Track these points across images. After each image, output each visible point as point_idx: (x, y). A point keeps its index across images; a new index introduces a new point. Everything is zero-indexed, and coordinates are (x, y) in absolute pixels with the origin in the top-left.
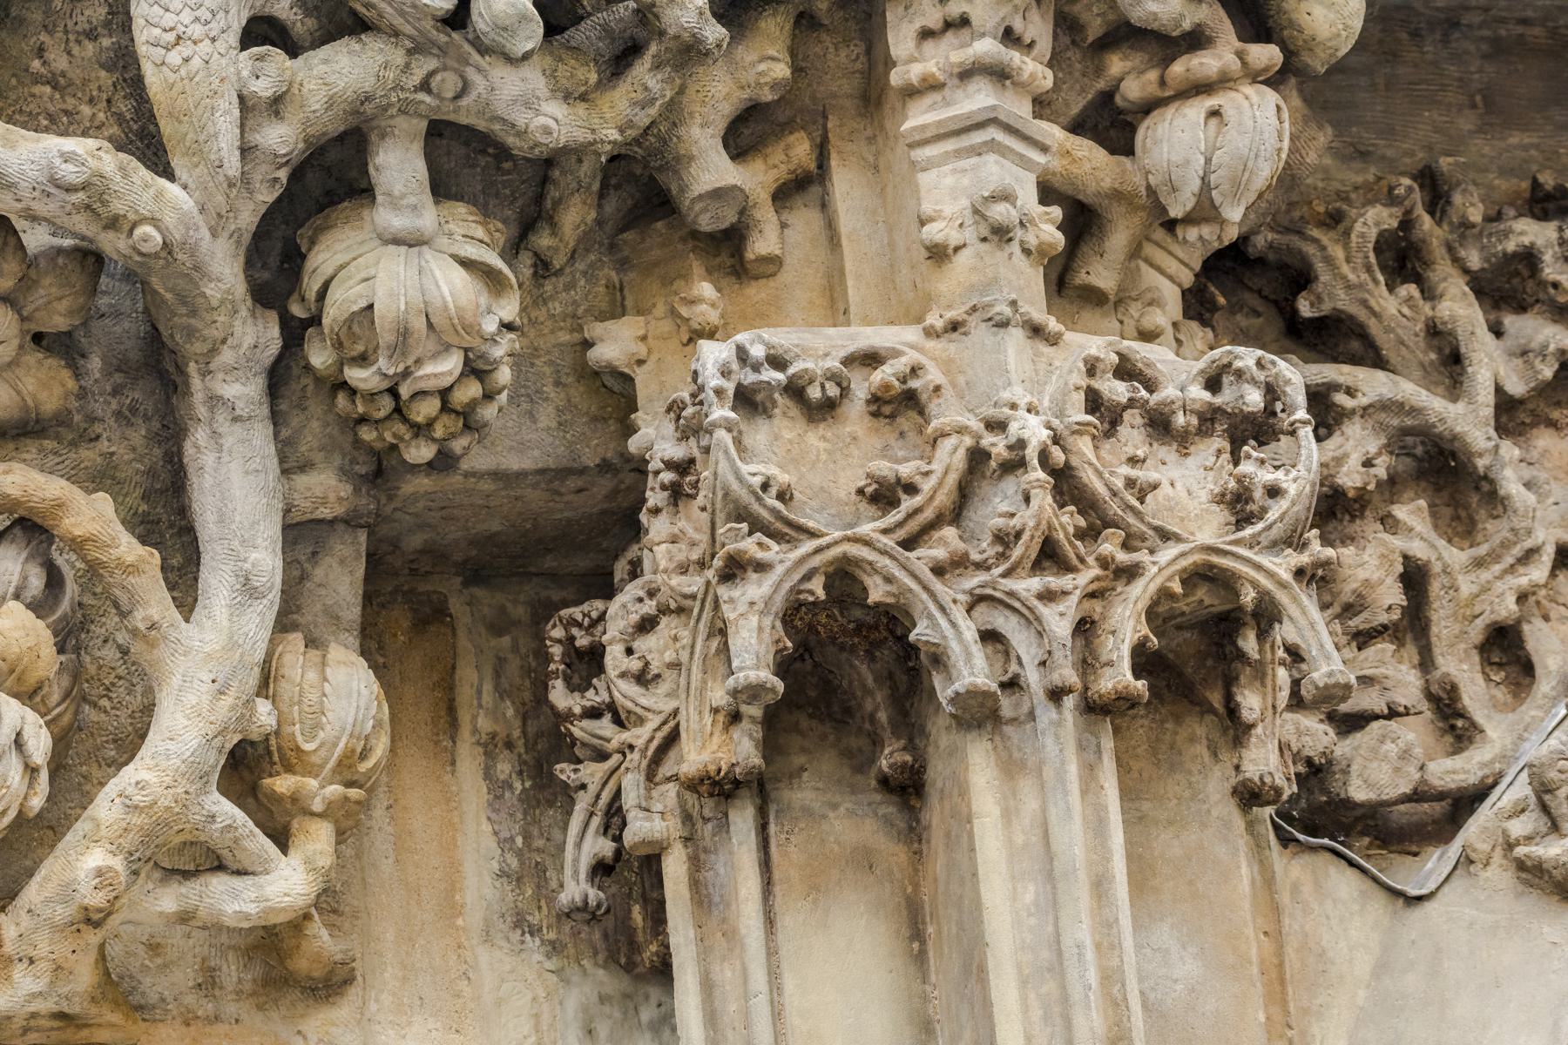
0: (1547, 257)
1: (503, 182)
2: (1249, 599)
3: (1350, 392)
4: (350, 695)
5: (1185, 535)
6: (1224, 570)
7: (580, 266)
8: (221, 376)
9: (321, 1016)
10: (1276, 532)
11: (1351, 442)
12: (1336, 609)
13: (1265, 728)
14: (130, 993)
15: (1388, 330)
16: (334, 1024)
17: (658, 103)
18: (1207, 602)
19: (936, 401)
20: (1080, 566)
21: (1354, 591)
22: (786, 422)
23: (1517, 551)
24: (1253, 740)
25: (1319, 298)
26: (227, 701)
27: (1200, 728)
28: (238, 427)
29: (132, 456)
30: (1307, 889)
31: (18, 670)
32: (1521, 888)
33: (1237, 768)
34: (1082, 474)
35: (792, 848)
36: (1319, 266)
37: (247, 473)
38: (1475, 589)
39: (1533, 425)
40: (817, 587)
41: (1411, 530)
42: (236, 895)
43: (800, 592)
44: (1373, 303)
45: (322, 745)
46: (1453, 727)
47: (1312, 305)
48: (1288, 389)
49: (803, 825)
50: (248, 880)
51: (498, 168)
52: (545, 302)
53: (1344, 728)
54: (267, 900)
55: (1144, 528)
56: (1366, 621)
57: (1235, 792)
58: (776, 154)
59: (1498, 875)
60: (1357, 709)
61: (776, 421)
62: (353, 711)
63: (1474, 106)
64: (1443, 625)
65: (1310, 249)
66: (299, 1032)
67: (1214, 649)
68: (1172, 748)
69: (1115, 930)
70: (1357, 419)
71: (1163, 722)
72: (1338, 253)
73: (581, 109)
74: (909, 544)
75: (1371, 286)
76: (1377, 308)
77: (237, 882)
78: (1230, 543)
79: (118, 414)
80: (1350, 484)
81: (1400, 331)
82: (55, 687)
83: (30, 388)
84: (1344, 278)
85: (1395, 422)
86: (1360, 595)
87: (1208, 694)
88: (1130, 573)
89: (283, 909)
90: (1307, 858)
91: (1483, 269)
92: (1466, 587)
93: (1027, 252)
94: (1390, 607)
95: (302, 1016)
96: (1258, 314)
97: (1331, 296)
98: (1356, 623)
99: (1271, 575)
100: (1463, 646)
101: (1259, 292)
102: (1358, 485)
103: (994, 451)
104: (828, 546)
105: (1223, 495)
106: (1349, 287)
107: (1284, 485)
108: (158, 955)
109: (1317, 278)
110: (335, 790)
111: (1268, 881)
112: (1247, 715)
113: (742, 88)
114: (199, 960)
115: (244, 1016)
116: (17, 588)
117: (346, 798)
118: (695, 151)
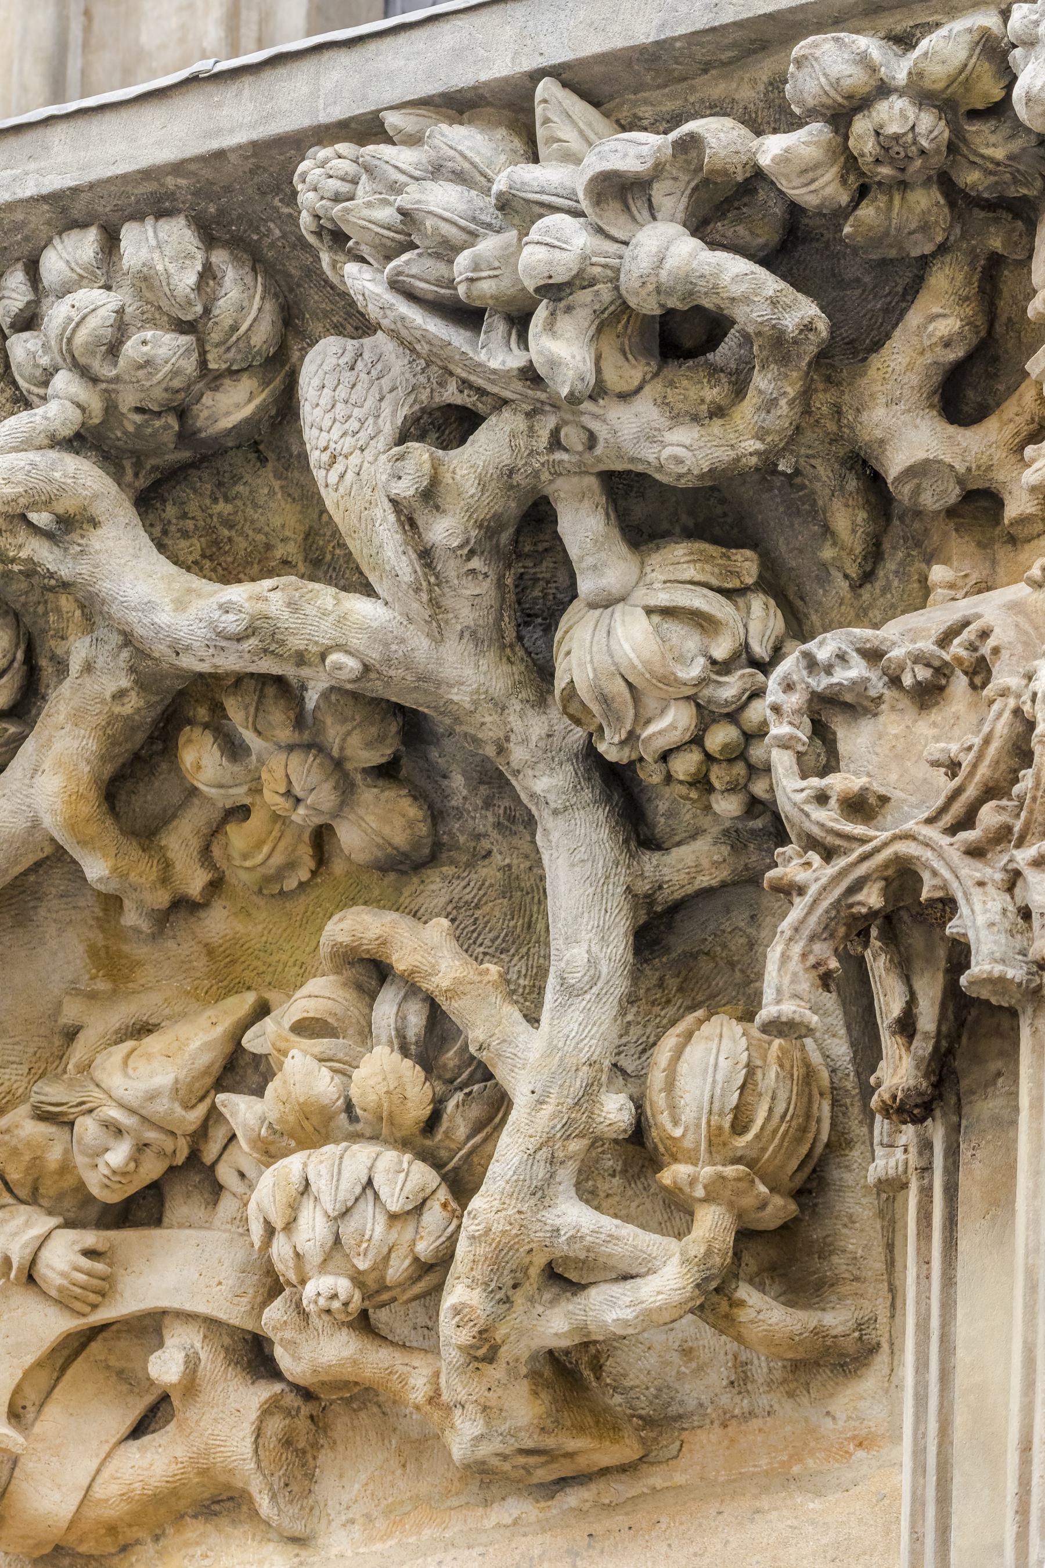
1: (800, 498)
4: (706, 1071)
7: (890, 565)
8: (530, 772)
9: (848, 1392)
14: (669, 1404)
16: (862, 1398)
17: (783, 402)
22: (893, 717)
26: (548, 1109)
28: (560, 821)
29: (528, 864)
31: (385, 1114)
35: (977, 1165)
37: (573, 865)
40: (872, 898)
42: (613, 1303)
43: (851, 906)
45: (686, 1130)
49: (990, 1137)
50: (629, 1284)
51: (791, 485)
52: (866, 614)
54: (642, 1302)
58: (1010, 408)
61: (882, 718)
62: (708, 1087)
66: (828, 1413)
73: (716, 426)
74: (952, 830)
77: (616, 1290)
79: (498, 825)
82: (459, 1120)
83: (374, 825)
89: (660, 1308)
95: (831, 1395)
104: (877, 850)
108: (691, 1360)
110: (707, 1171)
113: (922, 353)
114: (730, 1357)
115: (776, 1407)
116: (397, 1030)
117: (722, 1178)
118: (878, 434)
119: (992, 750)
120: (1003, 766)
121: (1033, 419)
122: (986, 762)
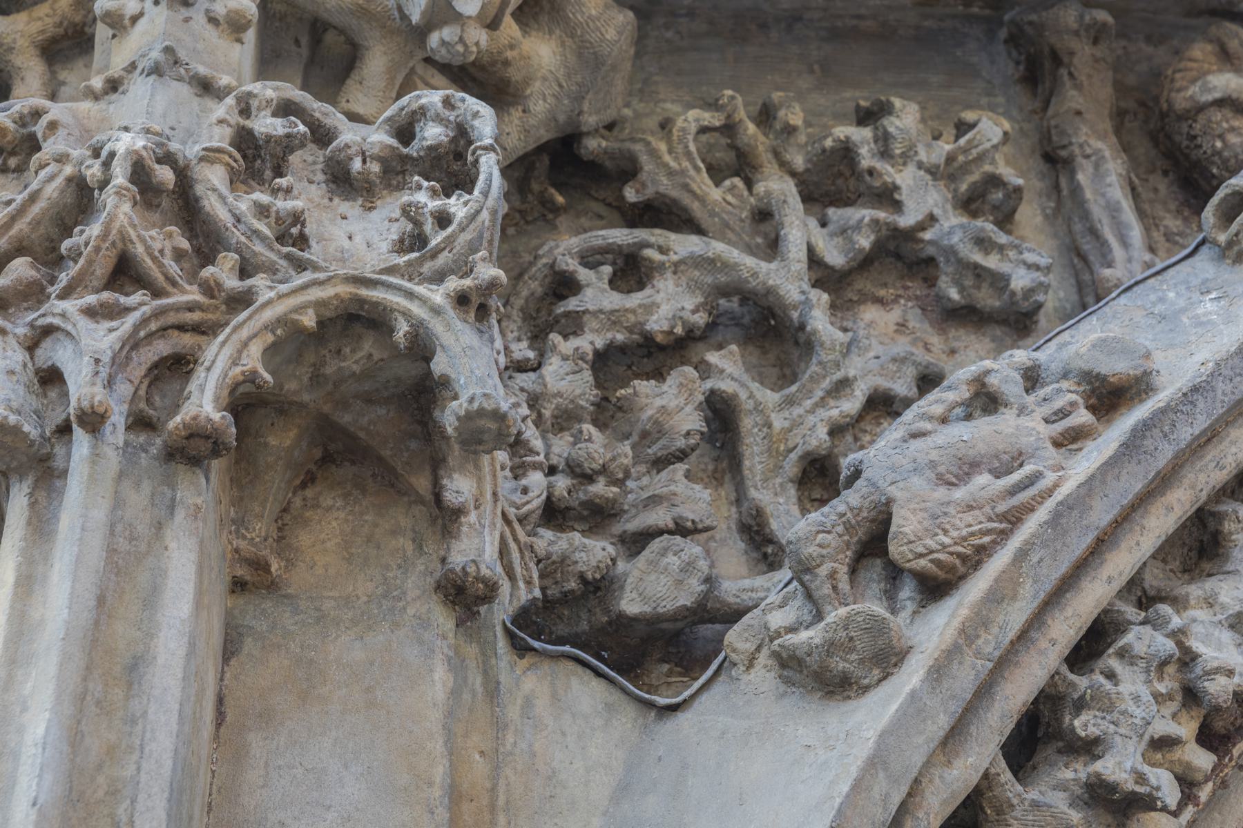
0: (864, 151)
2: (401, 334)
3: (663, 250)
5: (324, 264)
6: (376, 304)
10: (443, 259)
11: (662, 295)
12: (635, 438)
13: (479, 517)
15: (713, 214)
18: (376, 356)
19: (51, 140)
20: (170, 289)
21: (650, 418)
23: (826, 384)
24: (465, 529)
25: (644, 185)
27: (402, 517)
30: (542, 705)
32: (782, 688)
33: (443, 560)
34: (205, 203)
36: (644, 158)
38: (787, 424)
39: (860, 302)
41: (722, 371)
44: (694, 187)
46: (765, 556)
47: (637, 192)
48: (476, 123)
53: (633, 548)
55: (273, 257)
56: (664, 447)
57: (438, 587)
59: (763, 677)
60: (642, 526)
63: (812, 71)
64: (754, 459)
65: (638, 147)
67: (419, 429)
68: (369, 541)
69: (140, 727)
70: (669, 275)
71: (362, 514)
72: (663, 147)
75: (692, 172)
76: (698, 192)
78: (382, 272)
80: (656, 328)
81: (724, 216)
84: (666, 165)
85: (709, 279)
86: (656, 422)
87: (413, 480)
88: (241, 301)
90: (546, 666)
91: (807, 170)
92: (778, 422)
93: (213, 20)
94: (688, 433)
96: (600, 217)
97: (654, 182)
98: (654, 450)
99: (423, 301)
100: (779, 480)
101: (604, 201)
102: (665, 328)
103: (89, 173)
105: (402, 241)
106: (671, 173)
107: (452, 210)
109: (641, 168)
111: (493, 691)
112: (449, 497)
119: (36, 209)
120: (42, 230)
121: (61, 23)
122: (28, 218)
